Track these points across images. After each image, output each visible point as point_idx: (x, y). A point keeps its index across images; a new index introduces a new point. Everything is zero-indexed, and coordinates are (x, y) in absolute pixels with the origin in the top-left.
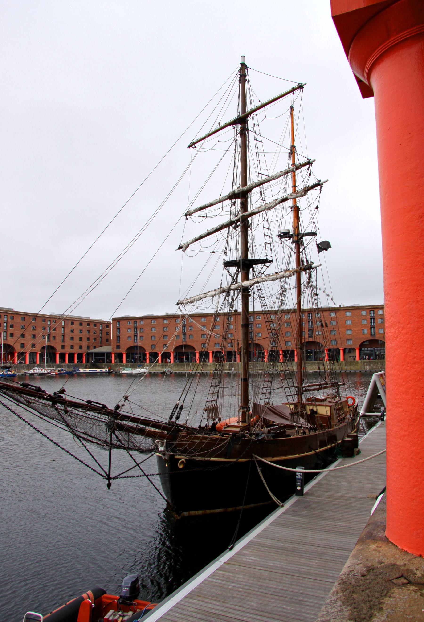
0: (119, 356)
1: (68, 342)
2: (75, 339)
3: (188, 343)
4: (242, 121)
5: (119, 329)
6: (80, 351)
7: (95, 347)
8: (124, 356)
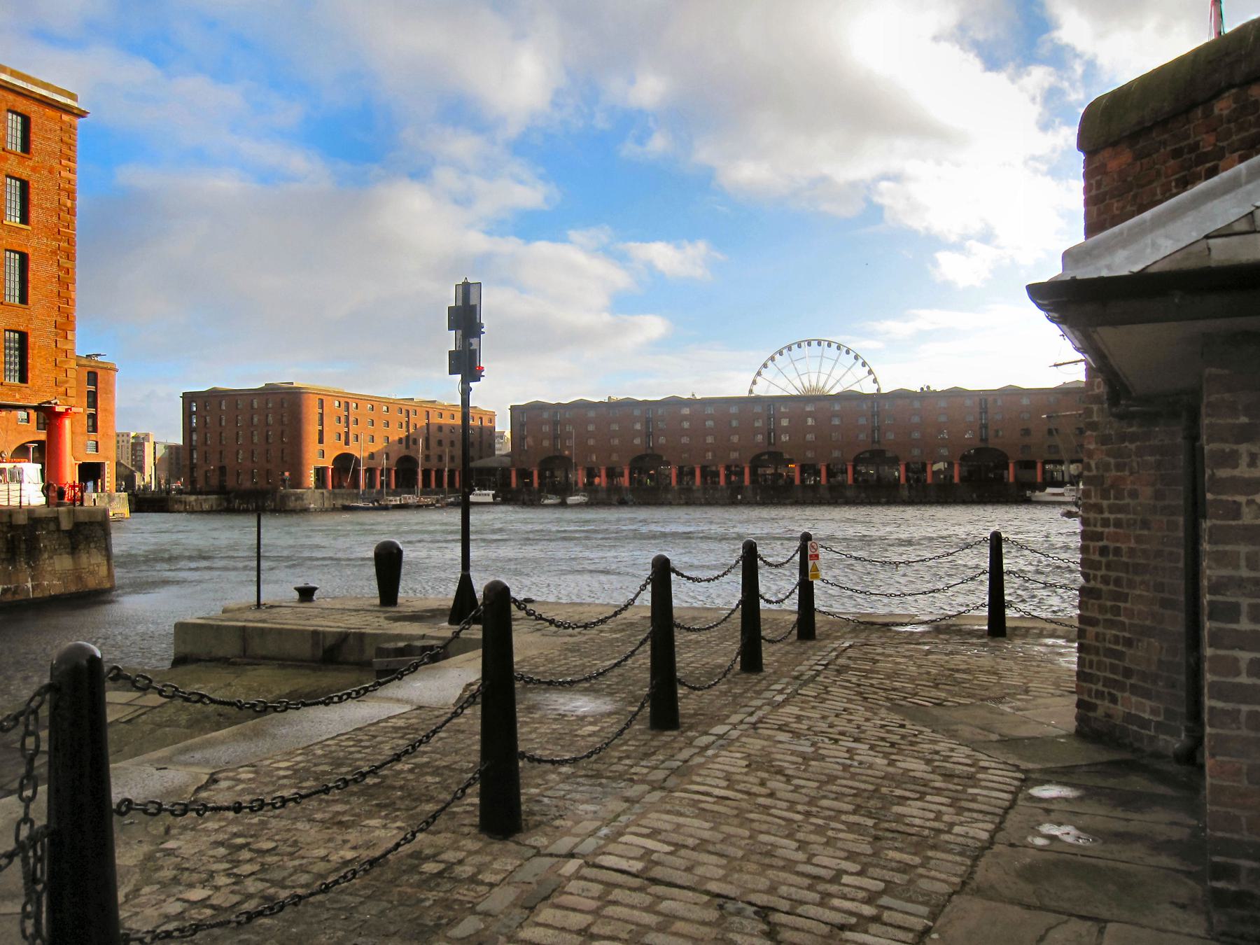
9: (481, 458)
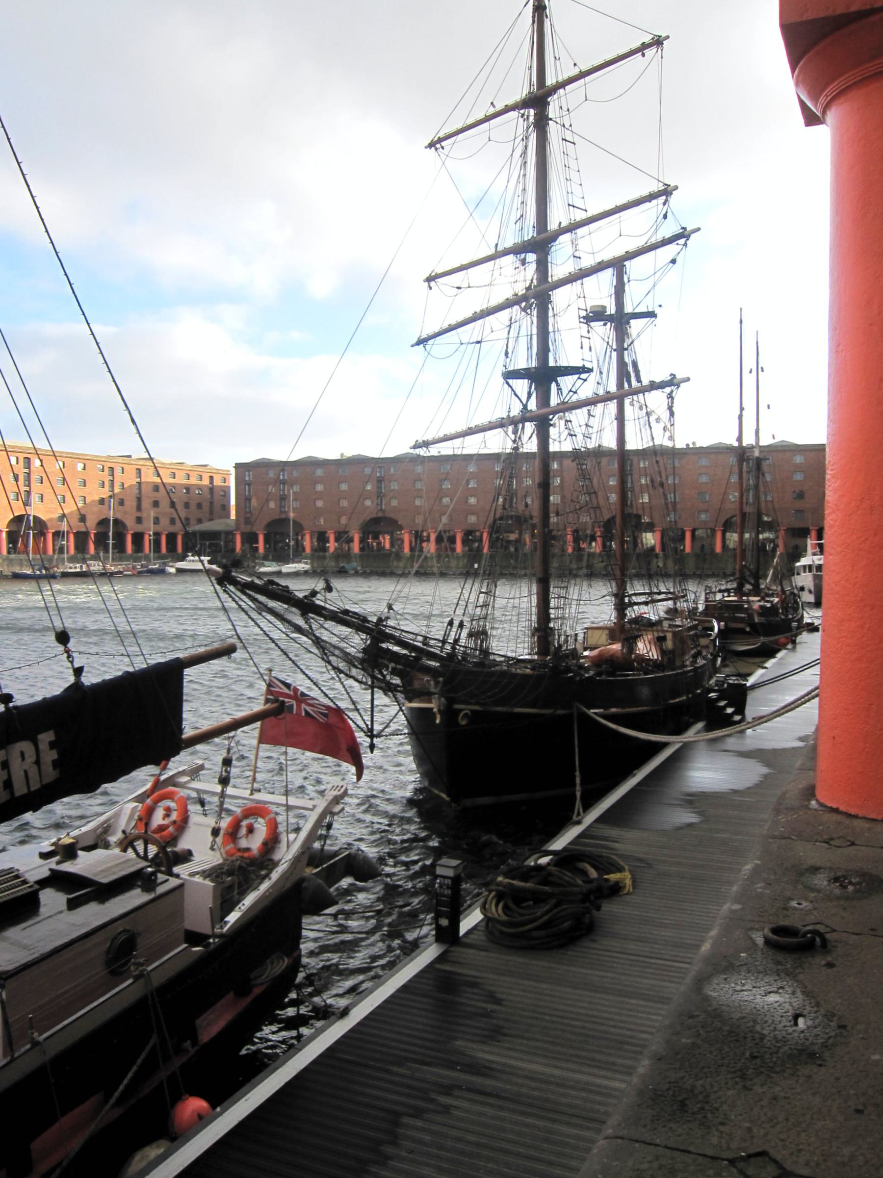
0: (250, 539)
1: (150, 513)
2: (161, 505)
3: (387, 515)
4: (538, 102)
5: (249, 485)
6: (172, 529)
7: (200, 521)
8: (261, 538)
9: (211, 520)
